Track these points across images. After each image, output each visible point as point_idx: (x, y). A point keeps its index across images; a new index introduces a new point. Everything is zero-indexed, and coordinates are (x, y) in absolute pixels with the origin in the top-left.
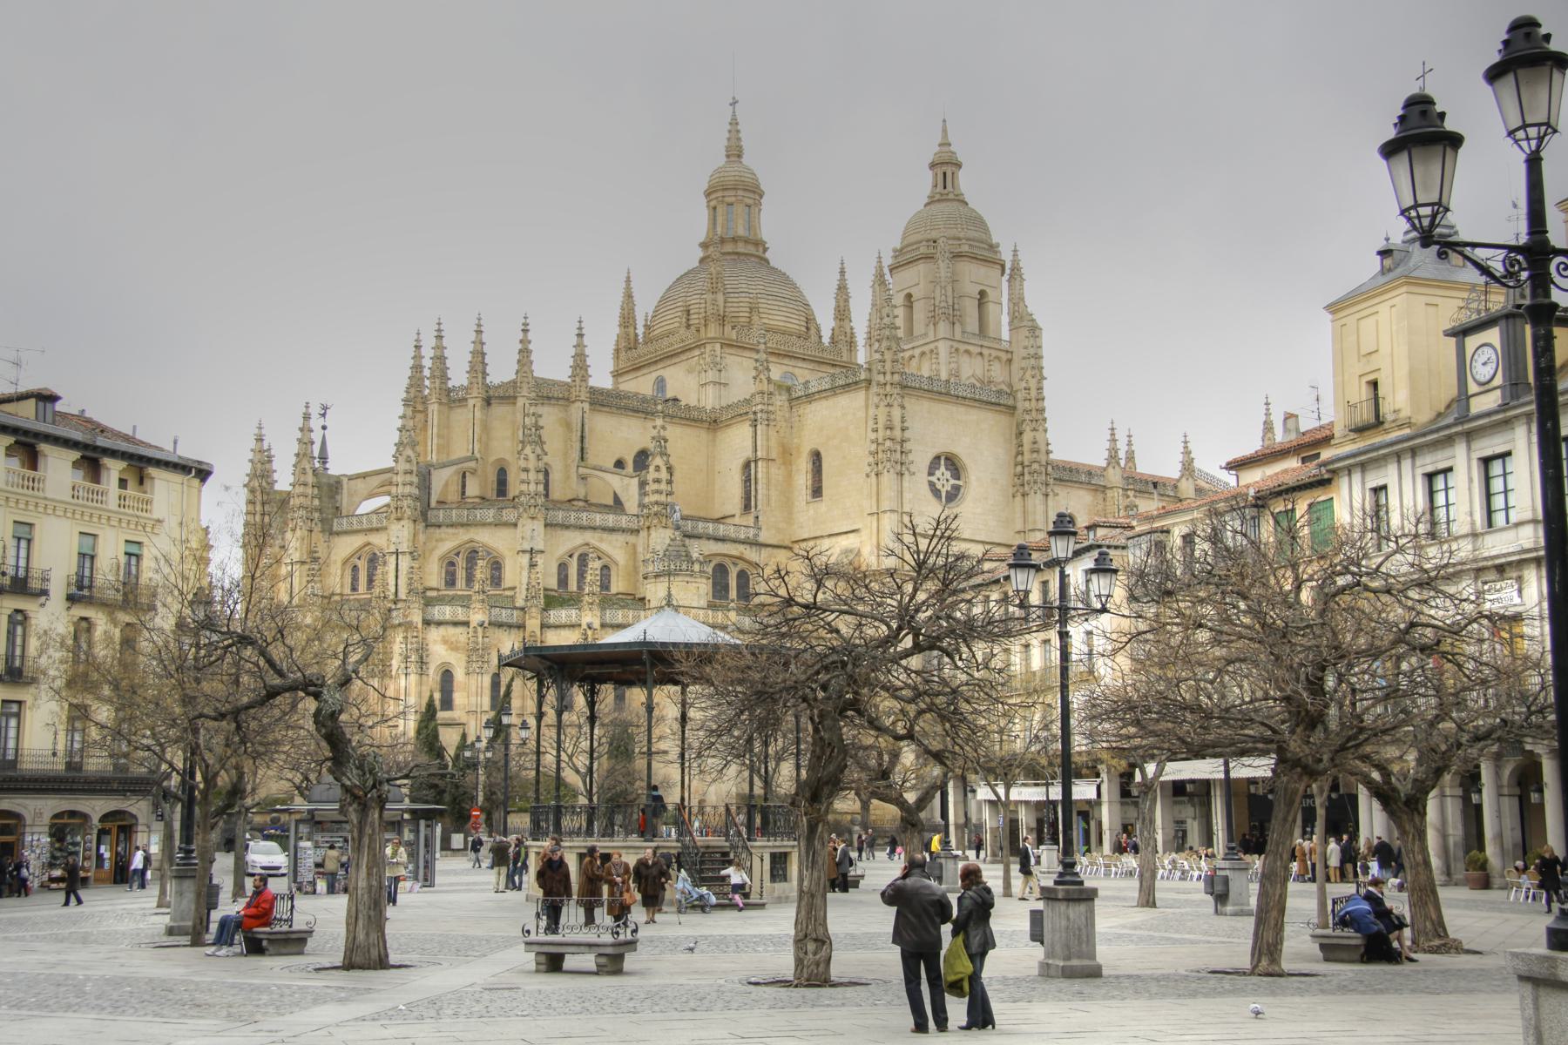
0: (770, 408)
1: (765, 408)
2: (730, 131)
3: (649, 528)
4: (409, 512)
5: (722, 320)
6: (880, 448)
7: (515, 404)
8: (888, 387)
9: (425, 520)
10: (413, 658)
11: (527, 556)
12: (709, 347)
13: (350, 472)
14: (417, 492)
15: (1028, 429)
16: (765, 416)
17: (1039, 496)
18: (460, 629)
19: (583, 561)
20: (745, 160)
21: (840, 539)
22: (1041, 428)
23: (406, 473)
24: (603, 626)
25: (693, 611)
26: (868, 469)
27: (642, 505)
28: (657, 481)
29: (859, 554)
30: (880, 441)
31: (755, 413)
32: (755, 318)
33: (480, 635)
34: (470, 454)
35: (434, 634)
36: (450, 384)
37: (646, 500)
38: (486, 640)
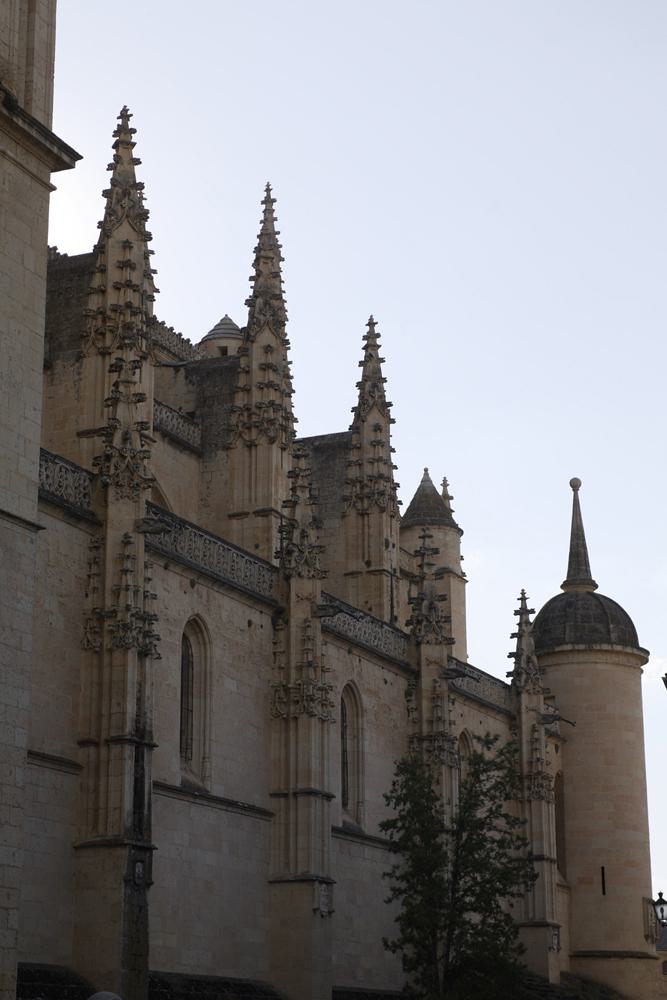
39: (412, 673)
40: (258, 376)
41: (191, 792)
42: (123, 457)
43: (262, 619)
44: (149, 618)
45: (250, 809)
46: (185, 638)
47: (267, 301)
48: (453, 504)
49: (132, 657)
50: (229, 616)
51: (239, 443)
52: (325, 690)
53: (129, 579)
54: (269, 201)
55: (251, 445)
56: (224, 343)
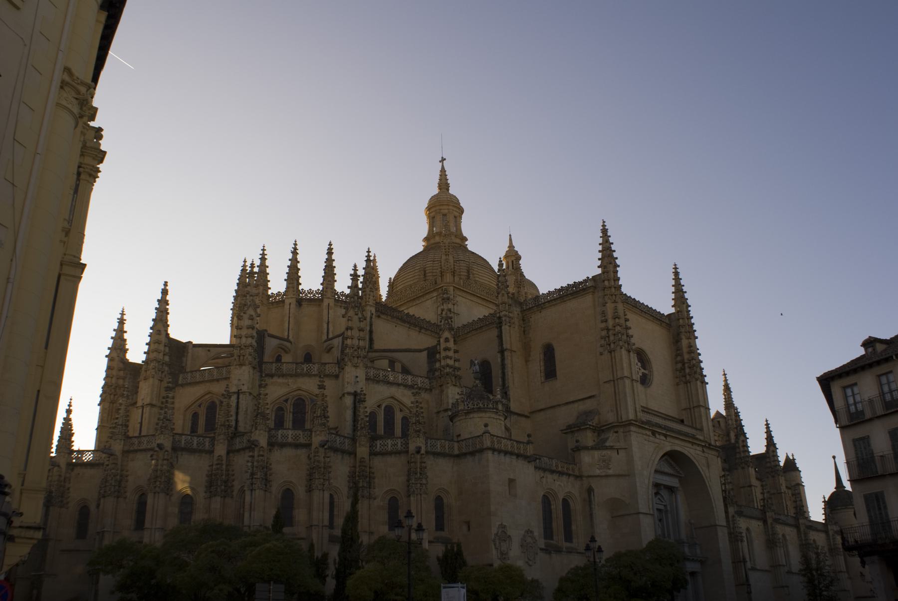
0: (510, 314)
1: (507, 313)
2: (441, 175)
3: (441, 386)
5: (454, 273)
6: (611, 332)
7: (320, 305)
8: (613, 290)
9: (261, 371)
13: (195, 341)
14: (255, 344)
15: (683, 337)
16: (508, 319)
17: (699, 383)
18: (302, 452)
19: (389, 411)
20: (450, 192)
21: (576, 405)
22: (692, 337)
23: (248, 327)
24: (427, 452)
25: (504, 441)
27: (432, 370)
28: (446, 349)
30: (610, 327)
34: (286, 337)
35: (278, 455)
36: (270, 292)
37: (437, 365)
38: (328, 459)
39: (797, 527)
40: (742, 449)
41: (753, 569)
42: (729, 497)
43: (760, 523)
44: (741, 533)
45: (766, 571)
46: (746, 534)
47: (729, 404)
48: (796, 461)
49: (740, 542)
50: (756, 526)
52: (779, 539)
53: (736, 525)
54: (725, 375)
55: (743, 468)
56: (718, 420)
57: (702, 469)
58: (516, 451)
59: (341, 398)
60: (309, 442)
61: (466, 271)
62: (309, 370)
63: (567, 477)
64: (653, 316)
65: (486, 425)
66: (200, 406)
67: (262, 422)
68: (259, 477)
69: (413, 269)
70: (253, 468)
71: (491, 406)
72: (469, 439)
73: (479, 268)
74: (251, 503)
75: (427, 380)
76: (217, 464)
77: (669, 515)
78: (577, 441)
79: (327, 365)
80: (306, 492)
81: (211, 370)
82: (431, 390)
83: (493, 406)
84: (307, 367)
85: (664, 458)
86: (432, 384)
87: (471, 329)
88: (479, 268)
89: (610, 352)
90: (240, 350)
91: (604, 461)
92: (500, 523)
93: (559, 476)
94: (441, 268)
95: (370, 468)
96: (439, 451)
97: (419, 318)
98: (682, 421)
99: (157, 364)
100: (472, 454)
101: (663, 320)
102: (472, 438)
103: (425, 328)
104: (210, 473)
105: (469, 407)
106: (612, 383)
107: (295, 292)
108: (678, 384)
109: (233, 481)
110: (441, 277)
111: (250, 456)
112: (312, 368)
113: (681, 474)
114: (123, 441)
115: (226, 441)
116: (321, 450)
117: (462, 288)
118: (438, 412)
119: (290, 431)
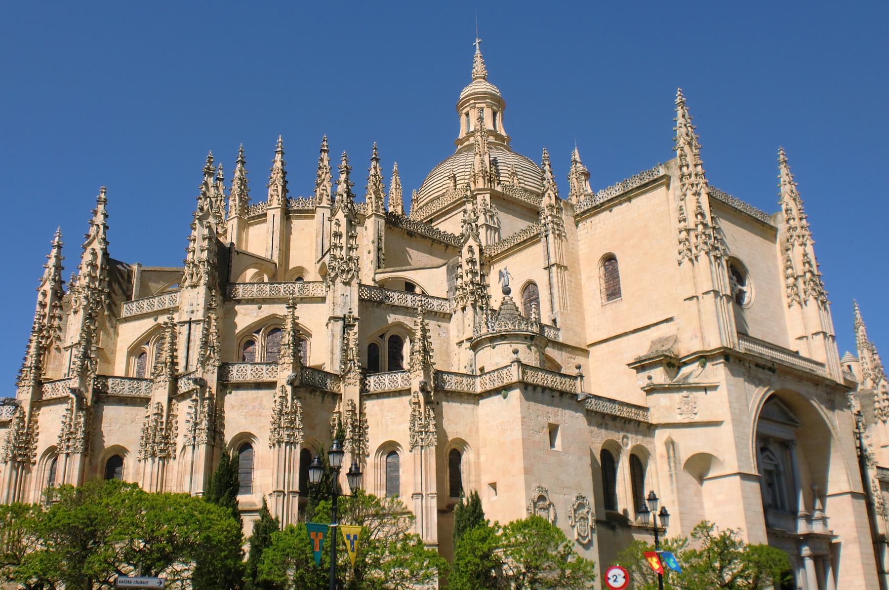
3: (464, 309)
4: (205, 279)
6: (692, 234)
7: (313, 217)
10: (204, 424)
11: (340, 324)
12: (479, 198)
15: (796, 243)
16: (555, 227)
19: (396, 344)
26: (680, 257)
29: (676, 341)
30: (692, 226)
31: (545, 225)
32: (516, 181)
33: (289, 398)
34: (269, 257)
37: (460, 281)
51: (880, 421)
56: (849, 363)
57: (826, 415)
58: (560, 388)
59: (327, 325)
60: (274, 380)
61: (507, 175)
62: (287, 292)
63: (637, 424)
64: (752, 217)
65: (516, 352)
66: (147, 344)
67: (210, 354)
68: (203, 427)
69: (442, 177)
70: (196, 415)
71: (523, 326)
72: (494, 371)
73: (524, 172)
74: (193, 462)
75: (444, 302)
76: (155, 414)
77: (783, 479)
78: (650, 378)
79: (311, 284)
80: (271, 447)
81: (162, 297)
82: (452, 315)
83: (528, 327)
84: (285, 288)
85: (772, 401)
86: (453, 307)
87: (512, 244)
88: (524, 172)
89: (691, 260)
90: (192, 267)
91: (687, 403)
92: (538, 485)
93: (625, 423)
94: (473, 172)
95: (361, 413)
96: (453, 388)
97: (444, 232)
98: (797, 352)
99: (89, 292)
100: (497, 391)
101: (765, 221)
102: (497, 370)
103: (452, 246)
104: (147, 426)
105: (493, 330)
106: (695, 299)
107: (280, 201)
108: (790, 306)
109: (176, 437)
110: (474, 182)
111: (193, 401)
112: (291, 288)
113: (797, 423)
114: (31, 387)
115: (168, 383)
116: (289, 389)
117: (501, 196)
118: (460, 344)
119: (249, 366)
